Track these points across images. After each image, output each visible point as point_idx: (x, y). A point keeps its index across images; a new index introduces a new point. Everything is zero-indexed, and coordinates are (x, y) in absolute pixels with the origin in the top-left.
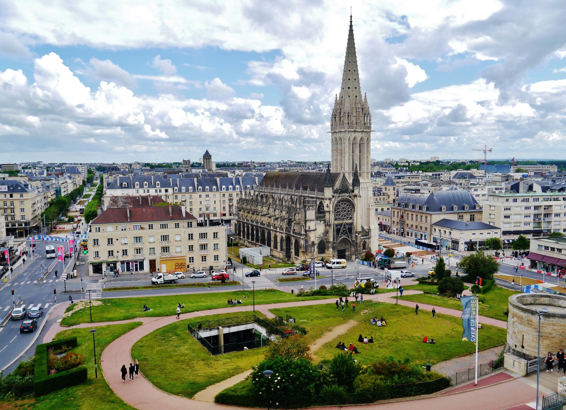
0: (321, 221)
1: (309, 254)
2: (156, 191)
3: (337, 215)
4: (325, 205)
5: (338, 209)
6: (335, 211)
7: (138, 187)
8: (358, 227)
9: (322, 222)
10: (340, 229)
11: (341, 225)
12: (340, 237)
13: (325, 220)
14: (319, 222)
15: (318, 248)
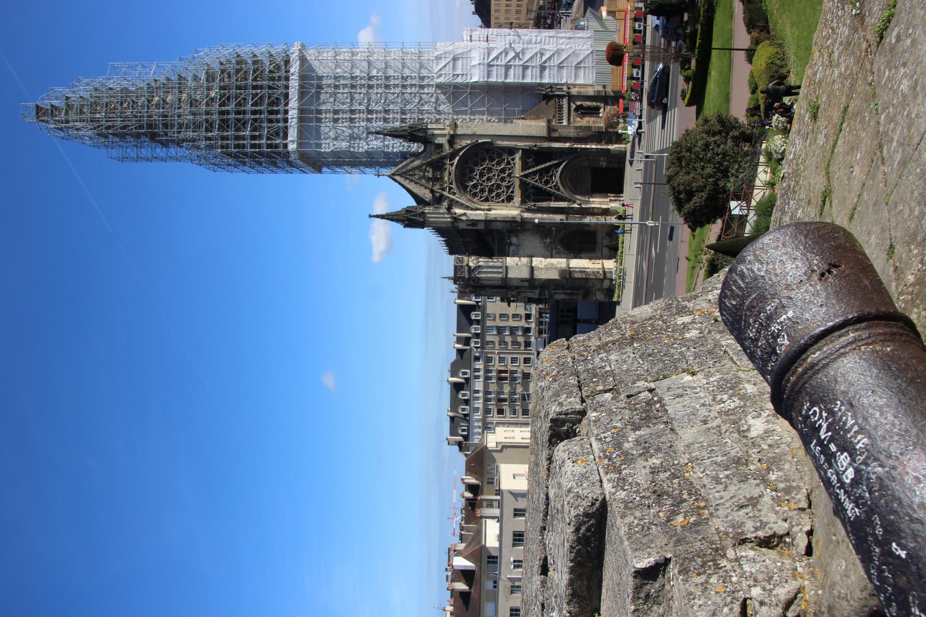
0: (511, 244)
1: (590, 283)
2: (478, 377)
3: (498, 195)
4: (470, 227)
5: (482, 191)
6: (487, 200)
7: (468, 407)
8: (534, 133)
9: (514, 240)
10: (534, 187)
11: (524, 186)
12: (558, 190)
13: (509, 231)
14: (512, 248)
15: (577, 253)
